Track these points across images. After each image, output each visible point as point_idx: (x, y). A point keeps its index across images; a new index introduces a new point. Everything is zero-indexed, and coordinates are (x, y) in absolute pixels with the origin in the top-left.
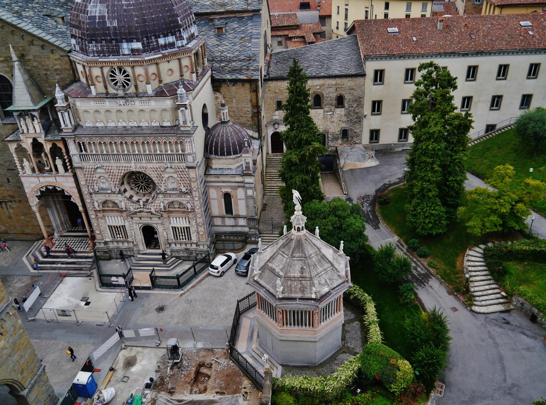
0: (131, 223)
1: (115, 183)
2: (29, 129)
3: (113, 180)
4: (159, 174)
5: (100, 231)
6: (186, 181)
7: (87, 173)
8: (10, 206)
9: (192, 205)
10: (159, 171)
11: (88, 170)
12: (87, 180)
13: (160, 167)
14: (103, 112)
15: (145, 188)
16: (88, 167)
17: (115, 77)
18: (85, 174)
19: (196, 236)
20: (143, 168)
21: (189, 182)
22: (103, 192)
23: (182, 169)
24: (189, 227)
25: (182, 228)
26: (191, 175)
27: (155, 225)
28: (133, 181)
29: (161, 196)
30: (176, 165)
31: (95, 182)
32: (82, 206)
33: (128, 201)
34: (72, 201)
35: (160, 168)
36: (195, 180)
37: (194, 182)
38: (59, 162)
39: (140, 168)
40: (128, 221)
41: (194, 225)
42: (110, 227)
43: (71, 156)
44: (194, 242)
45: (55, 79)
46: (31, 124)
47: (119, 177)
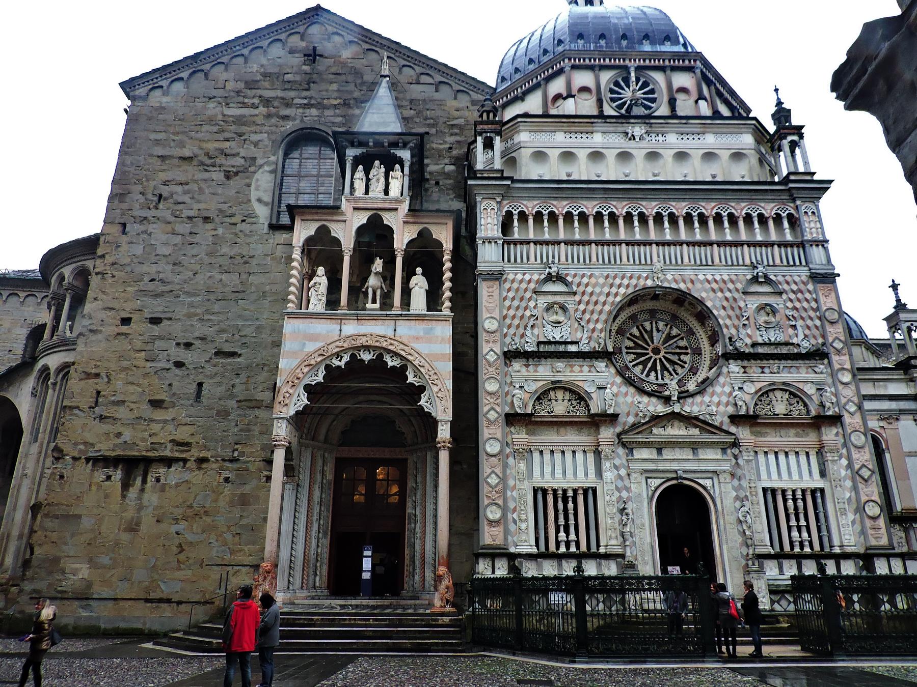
0: (623, 472)
1: (591, 326)
2: (371, 188)
3: (587, 316)
4: (731, 300)
5: (504, 509)
6: (811, 319)
7: (511, 295)
8: (158, 480)
9: (834, 400)
10: (730, 291)
11: (515, 285)
12: (505, 317)
13: (734, 278)
14: (582, 154)
15: (664, 368)
16: (519, 277)
17: (620, 94)
18: (505, 299)
19: (853, 522)
20: (684, 282)
21: (818, 323)
22: (552, 348)
23: (795, 283)
24: (822, 491)
25: (799, 494)
26: (822, 302)
27: (707, 483)
28: (637, 334)
29: (734, 367)
30: (780, 271)
31: (531, 323)
32: (451, 422)
33: (624, 389)
34: (421, 408)
35: (732, 281)
36: (836, 316)
37: (832, 323)
38: (419, 284)
39: (676, 281)
40: (616, 467)
41: (845, 478)
42: (540, 493)
43: (479, 242)
44: (849, 550)
45: (445, 142)
46: (382, 180)
47: (607, 308)
